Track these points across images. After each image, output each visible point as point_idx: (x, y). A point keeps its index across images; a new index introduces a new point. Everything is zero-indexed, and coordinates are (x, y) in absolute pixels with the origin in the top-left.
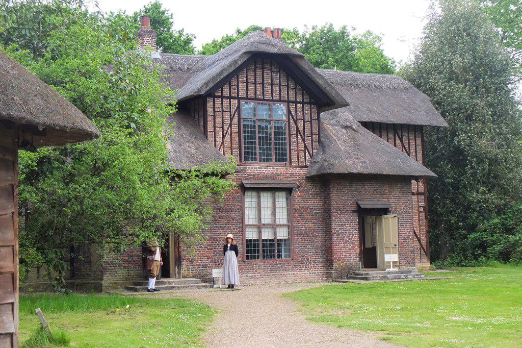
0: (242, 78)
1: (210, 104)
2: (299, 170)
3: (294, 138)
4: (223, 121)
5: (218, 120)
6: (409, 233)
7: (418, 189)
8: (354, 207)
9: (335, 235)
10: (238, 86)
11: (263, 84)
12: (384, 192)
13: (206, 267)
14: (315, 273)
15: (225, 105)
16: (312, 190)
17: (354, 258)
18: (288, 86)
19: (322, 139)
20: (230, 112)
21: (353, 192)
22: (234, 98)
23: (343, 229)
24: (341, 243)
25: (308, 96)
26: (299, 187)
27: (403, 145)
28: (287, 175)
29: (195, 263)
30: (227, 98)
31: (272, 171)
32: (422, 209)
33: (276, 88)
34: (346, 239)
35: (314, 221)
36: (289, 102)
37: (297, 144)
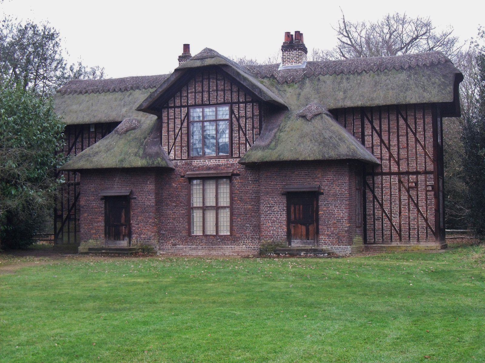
3: (236, 134)
7: (426, 168)
9: (262, 215)
10: (187, 96)
12: (316, 176)
14: (251, 248)
15: (177, 113)
20: (181, 118)
21: (283, 177)
22: (184, 107)
23: (271, 210)
24: (269, 223)
28: (228, 165)
31: (214, 163)
32: (430, 188)
33: (221, 93)
35: (253, 203)
37: (239, 138)
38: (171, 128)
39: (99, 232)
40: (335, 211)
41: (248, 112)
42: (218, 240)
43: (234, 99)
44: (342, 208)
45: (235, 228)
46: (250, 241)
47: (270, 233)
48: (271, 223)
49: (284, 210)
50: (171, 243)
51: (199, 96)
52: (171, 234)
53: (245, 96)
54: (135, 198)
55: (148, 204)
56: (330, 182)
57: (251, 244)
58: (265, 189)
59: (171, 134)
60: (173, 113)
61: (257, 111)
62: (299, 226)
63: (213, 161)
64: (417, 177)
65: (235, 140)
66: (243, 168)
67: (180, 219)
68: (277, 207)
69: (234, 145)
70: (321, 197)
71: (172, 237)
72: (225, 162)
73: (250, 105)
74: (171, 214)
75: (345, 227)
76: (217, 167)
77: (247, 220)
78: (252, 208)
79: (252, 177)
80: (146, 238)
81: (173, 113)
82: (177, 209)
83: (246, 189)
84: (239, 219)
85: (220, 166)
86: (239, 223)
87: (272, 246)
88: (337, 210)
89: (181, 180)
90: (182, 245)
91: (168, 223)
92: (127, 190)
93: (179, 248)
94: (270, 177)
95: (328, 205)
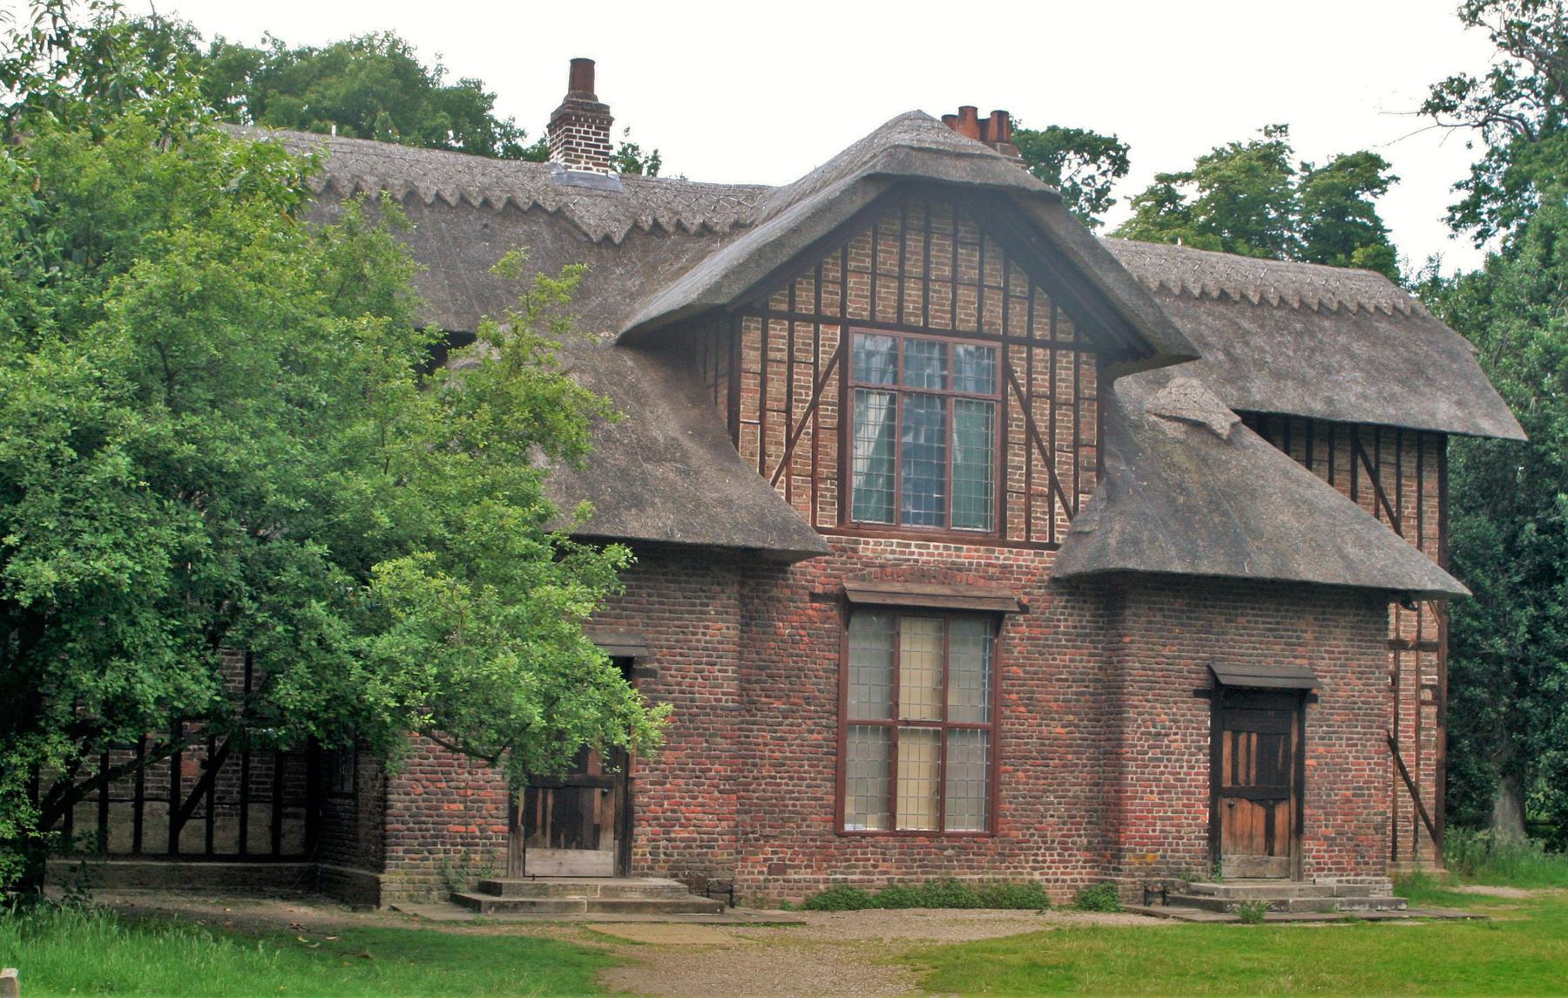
0: (860, 259)
1: (750, 338)
2: (1028, 554)
3: (1018, 455)
4: (790, 393)
5: (777, 388)
6: (1371, 770)
7: (1419, 632)
8: (1200, 681)
9: (1132, 766)
10: (843, 284)
11: (925, 280)
12: (1298, 638)
13: (713, 847)
14: (1064, 881)
16: (1066, 619)
17: (1189, 839)
18: (1006, 290)
19: (1108, 463)
20: (816, 364)
21: (1198, 632)
22: (830, 321)
23: (1160, 747)
24: (1152, 792)
25: (1069, 326)
26: (1024, 609)
27: (1380, 494)
28: (991, 570)
29: (678, 833)
30: (806, 319)
31: (940, 555)
32: (1427, 695)
33: (967, 295)
34: (1167, 780)
36: (1007, 340)
37: (1029, 474)
38: (776, 400)
39: (479, 809)
40: (1347, 758)
41: (1061, 380)
42: (946, 853)
43: (1014, 326)
44: (1370, 752)
45: (1007, 808)
46: (1056, 857)
47: (1154, 831)
48: (1160, 793)
49: (1200, 749)
50: (766, 860)
51: (887, 291)
52: (764, 826)
53: (1054, 318)
54: (652, 673)
55: (709, 700)
56: (1338, 662)
57: (1058, 868)
58: (1144, 669)
59: (774, 423)
60: (783, 337)
61: (1092, 383)
62: (1246, 805)
63: (937, 548)
64: (1396, 659)
65: (1013, 480)
66: (1040, 588)
67: (802, 766)
68: (1178, 737)
69: (1011, 497)
70: (1313, 711)
71: (767, 838)
72: (979, 557)
73: (1066, 356)
74: (766, 745)
75: (1375, 814)
76: (949, 573)
77: (1046, 778)
78: (1065, 736)
79: (1070, 623)
80: (695, 840)
81: (783, 337)
82: (791, 725)
83: (1050, 666)
84: (1020, 774)
85: (960, 570)
86: (1021, 787)
87: (1159, 875)
88: (1355, 757)
89: (811, 612)
90: (809, 870)
91: (755, 778)
92: (616, 632)
93: (799, 881)
94: (1160, 630)
95: (1330, 739)
